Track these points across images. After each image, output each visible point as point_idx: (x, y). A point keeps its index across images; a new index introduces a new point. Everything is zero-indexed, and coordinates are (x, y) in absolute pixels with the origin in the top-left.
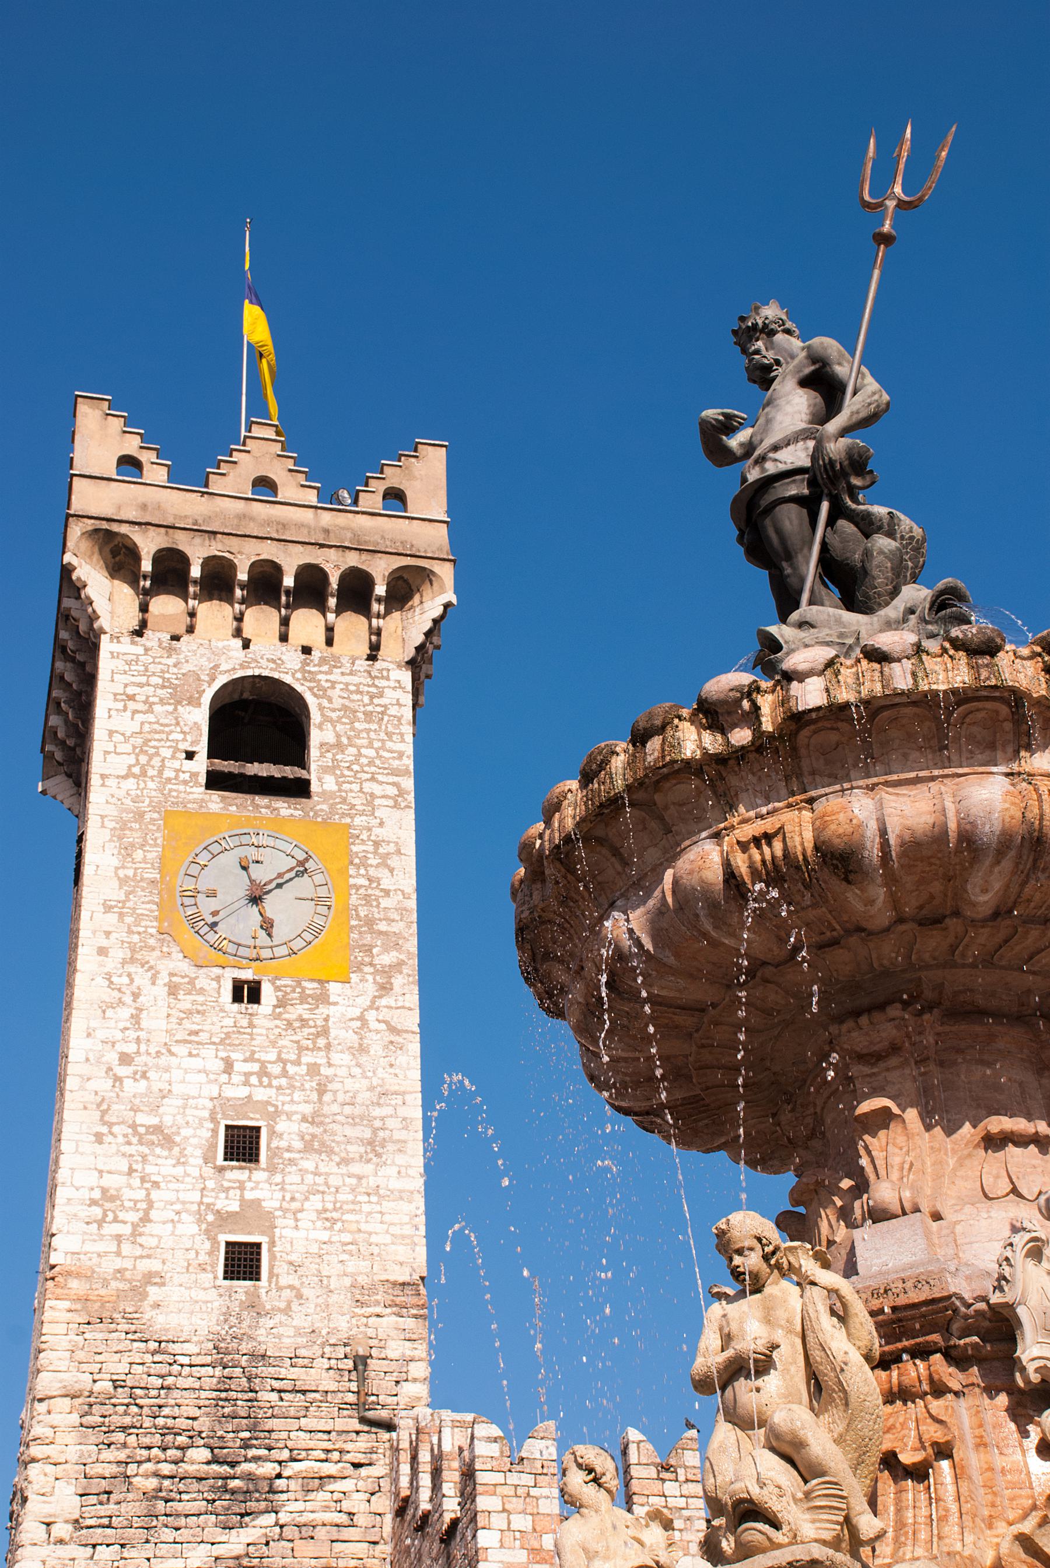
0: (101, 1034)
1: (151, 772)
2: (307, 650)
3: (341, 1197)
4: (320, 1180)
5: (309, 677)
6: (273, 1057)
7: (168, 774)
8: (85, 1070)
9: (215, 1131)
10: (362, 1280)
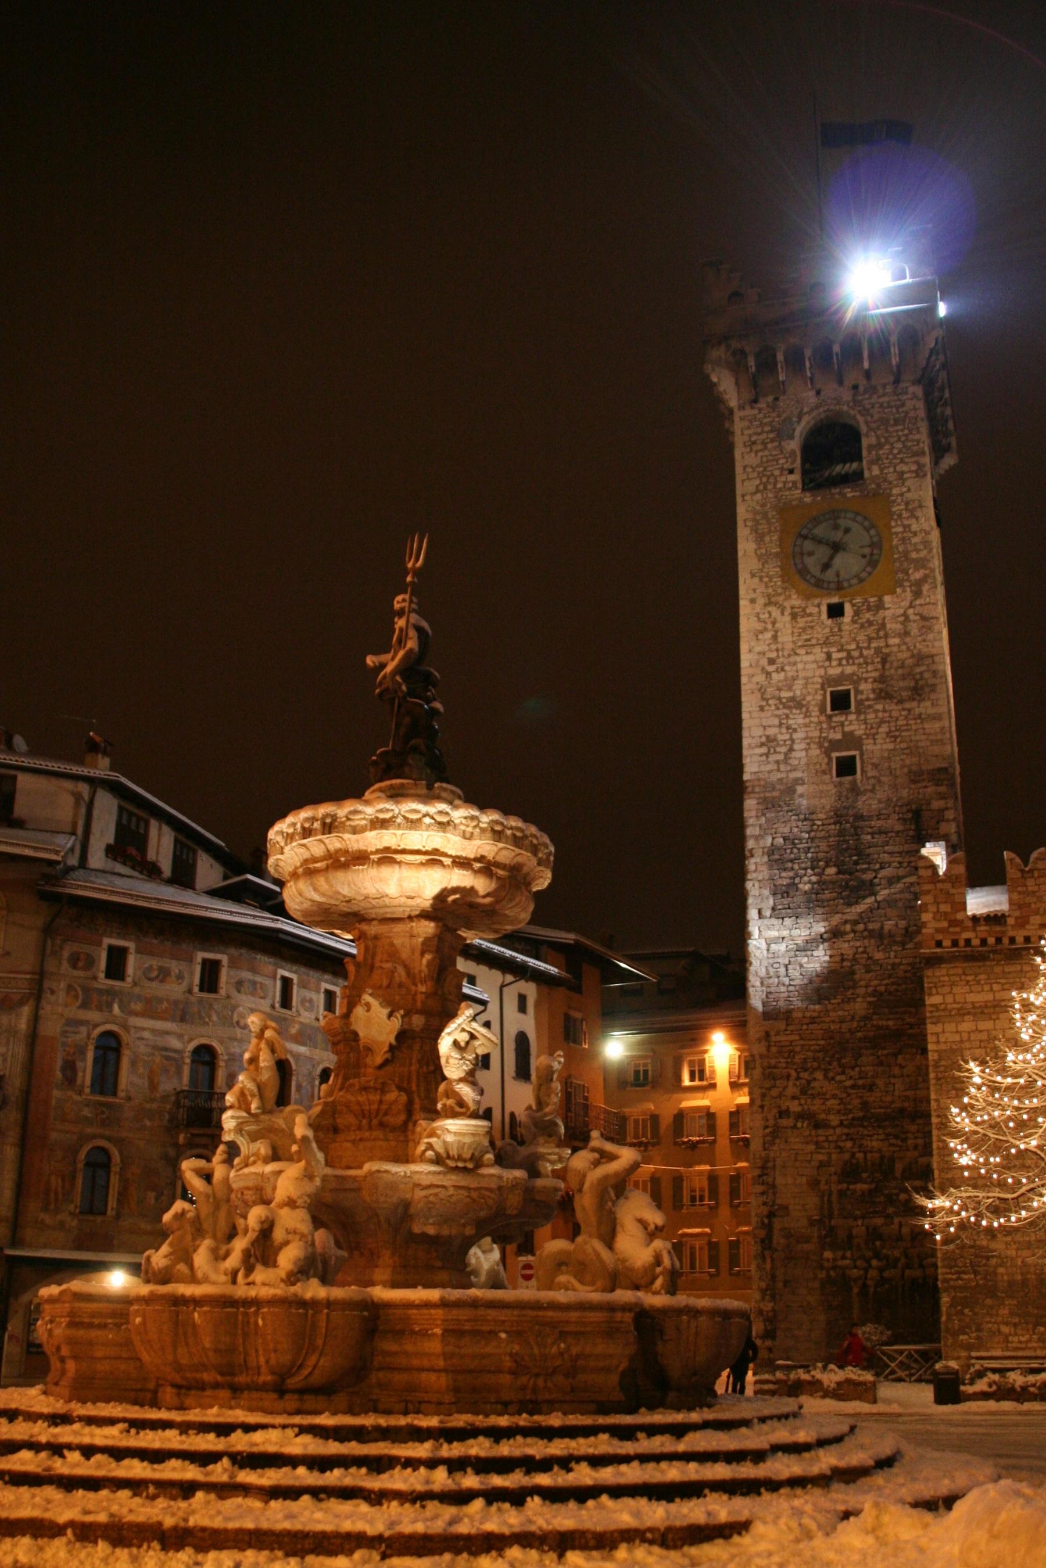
0: (758, 649)
1: (769, 487)
3: (900, 723)
4: (887, 715)
6: (853, 646)
7: (779, 485)
8: (750, 671)
9: (824, 696)
10: (914, 768)
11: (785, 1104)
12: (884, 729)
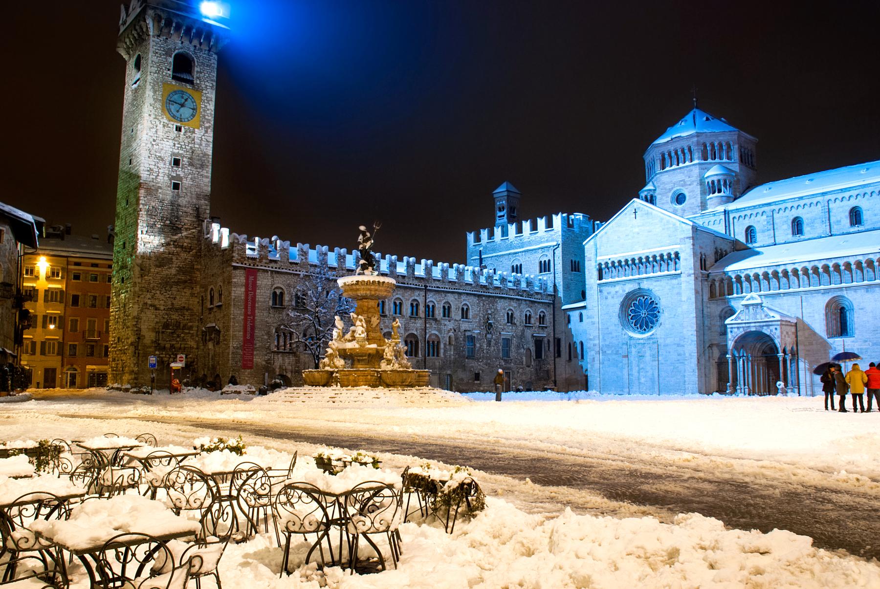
2: (195, 46)
5: (195, 53)
11: (146, 301)
12: (190, 176)
